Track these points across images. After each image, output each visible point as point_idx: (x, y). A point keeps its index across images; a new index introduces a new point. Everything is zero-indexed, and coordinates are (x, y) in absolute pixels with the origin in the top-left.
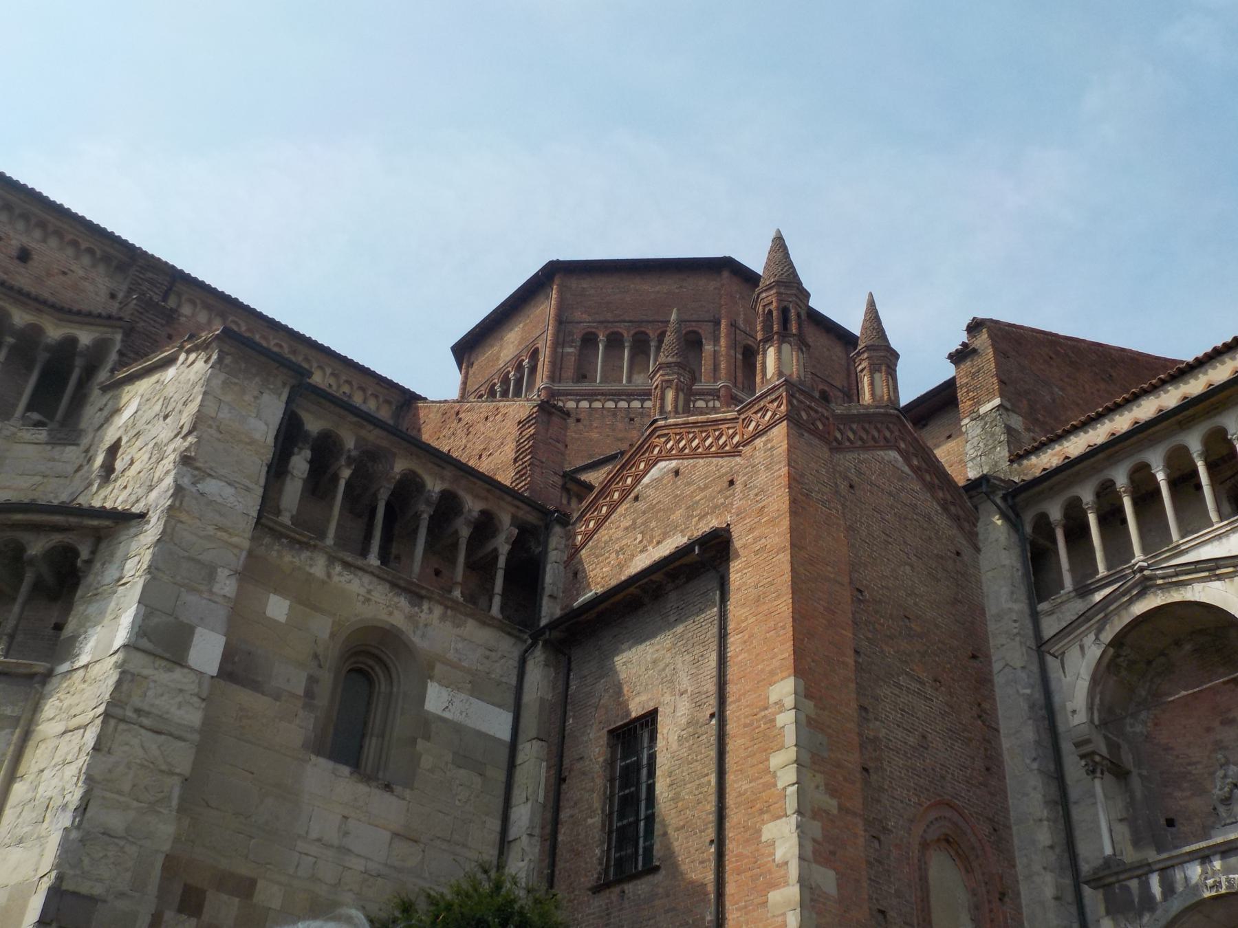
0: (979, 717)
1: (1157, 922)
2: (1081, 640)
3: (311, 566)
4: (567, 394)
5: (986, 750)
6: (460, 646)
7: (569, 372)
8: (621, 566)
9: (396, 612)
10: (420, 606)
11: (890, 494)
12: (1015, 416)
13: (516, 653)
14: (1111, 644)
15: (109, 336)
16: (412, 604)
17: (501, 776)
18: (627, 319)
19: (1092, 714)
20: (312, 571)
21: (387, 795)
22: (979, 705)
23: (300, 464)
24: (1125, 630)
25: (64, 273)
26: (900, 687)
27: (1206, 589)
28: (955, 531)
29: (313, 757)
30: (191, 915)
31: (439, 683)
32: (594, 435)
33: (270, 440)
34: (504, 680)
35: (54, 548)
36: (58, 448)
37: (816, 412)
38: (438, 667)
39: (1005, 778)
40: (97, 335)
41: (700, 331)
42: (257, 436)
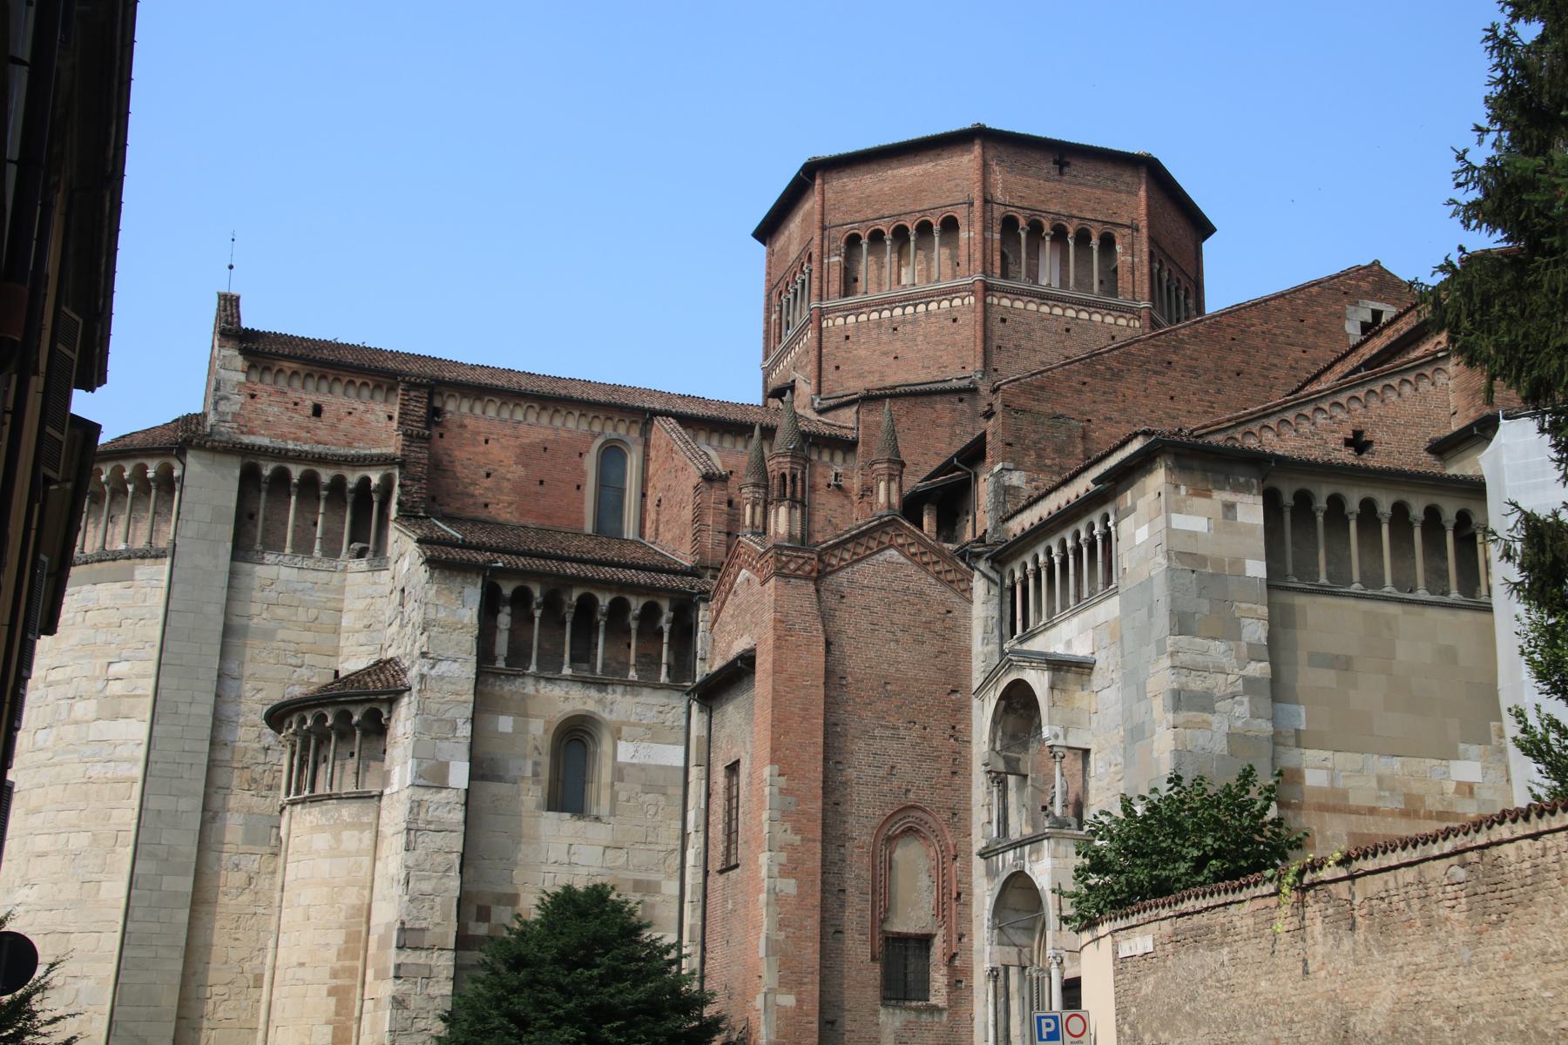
0: (951, 736)
3: (524, 688)
4: (836, 310)
5: (955, 760)
6: (639, 710)
7: (835, 285)
8: (730, 644)
9: (588, 700)
10: (606, 691)
11: (882, 588)
12: (1017, 473)
13: (684, 703)
14: (1001, 698)
15: (390, 471)
16: (600, 691)
17: (680, 791)
18: (887, 213)
19: (995, 743)
20: (525, 691)
21: (598, 824)
22: (954, 728)
23: (504, 619)
25: (350, 413)
26: (874, 738)
28: (950, 594)
29: (545, 814)
30: (484, 922)
31: (626, 741)
32: (863, 352)
33: (475, 620)
34: (676, 724)
35: (368, 711)
36: (376, 573)
37: (803, 558)
38: (625, 730)
39: (970, 775)
40: (382, 472)
41: (956, 215)
42: (466, 620)
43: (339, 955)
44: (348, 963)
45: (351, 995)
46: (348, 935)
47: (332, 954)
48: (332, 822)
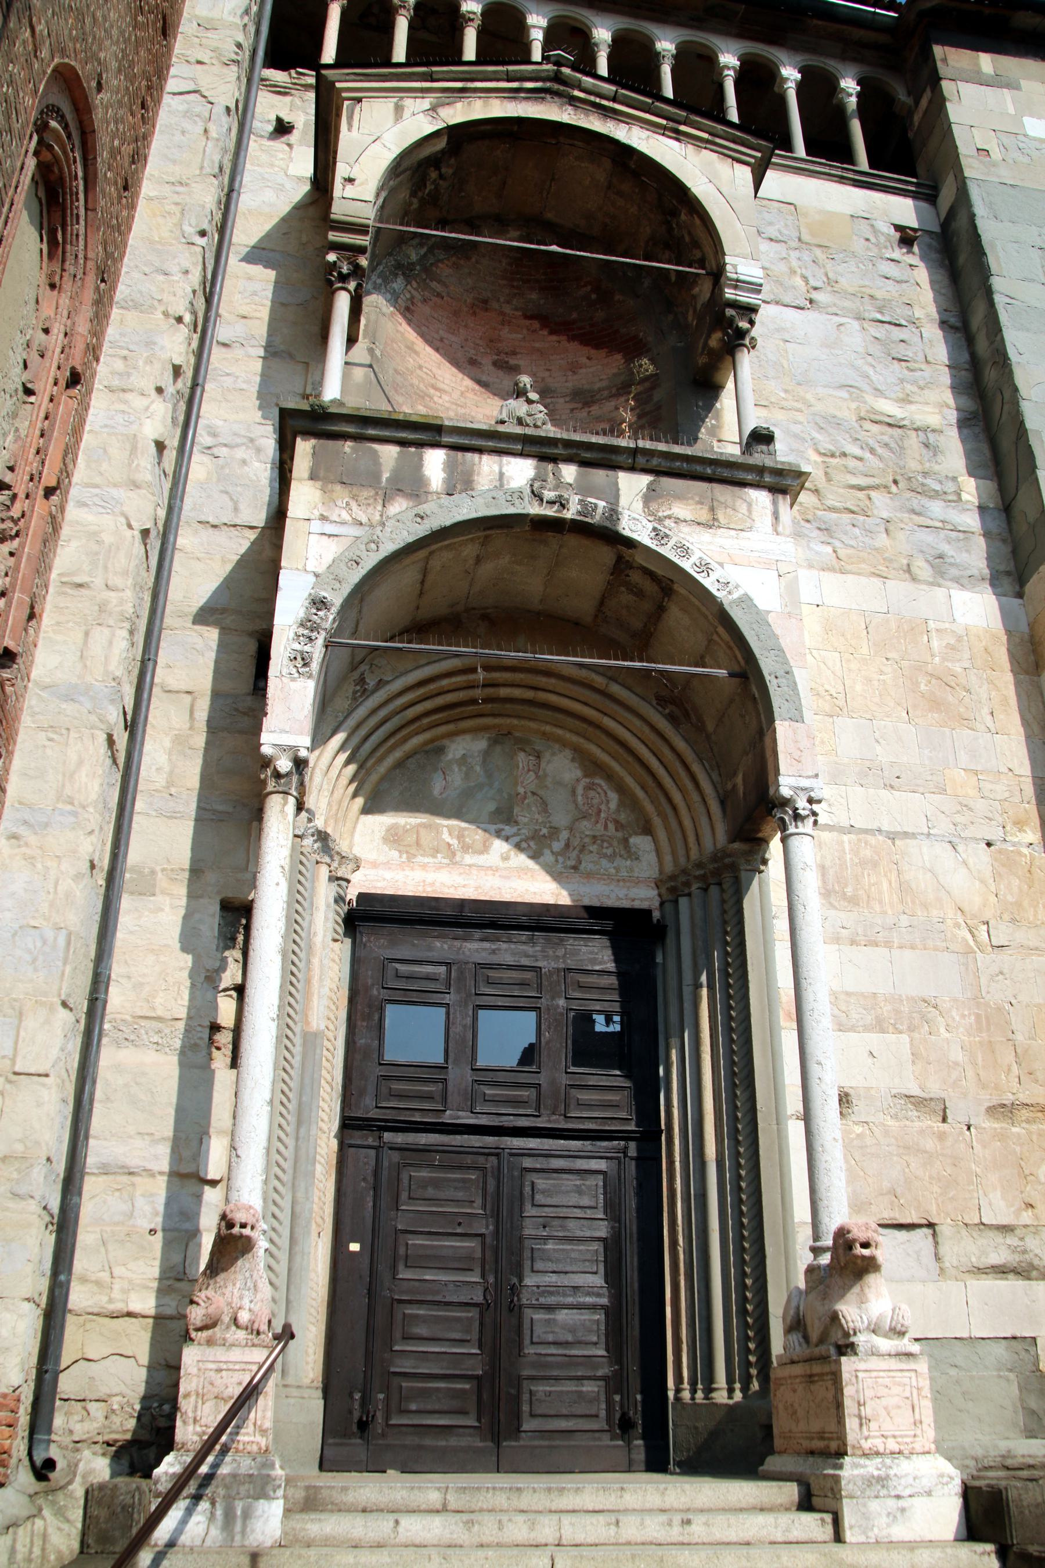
1: (419, 520)
2: (402, 98)
24: (483, 128)
27: (651, 141)
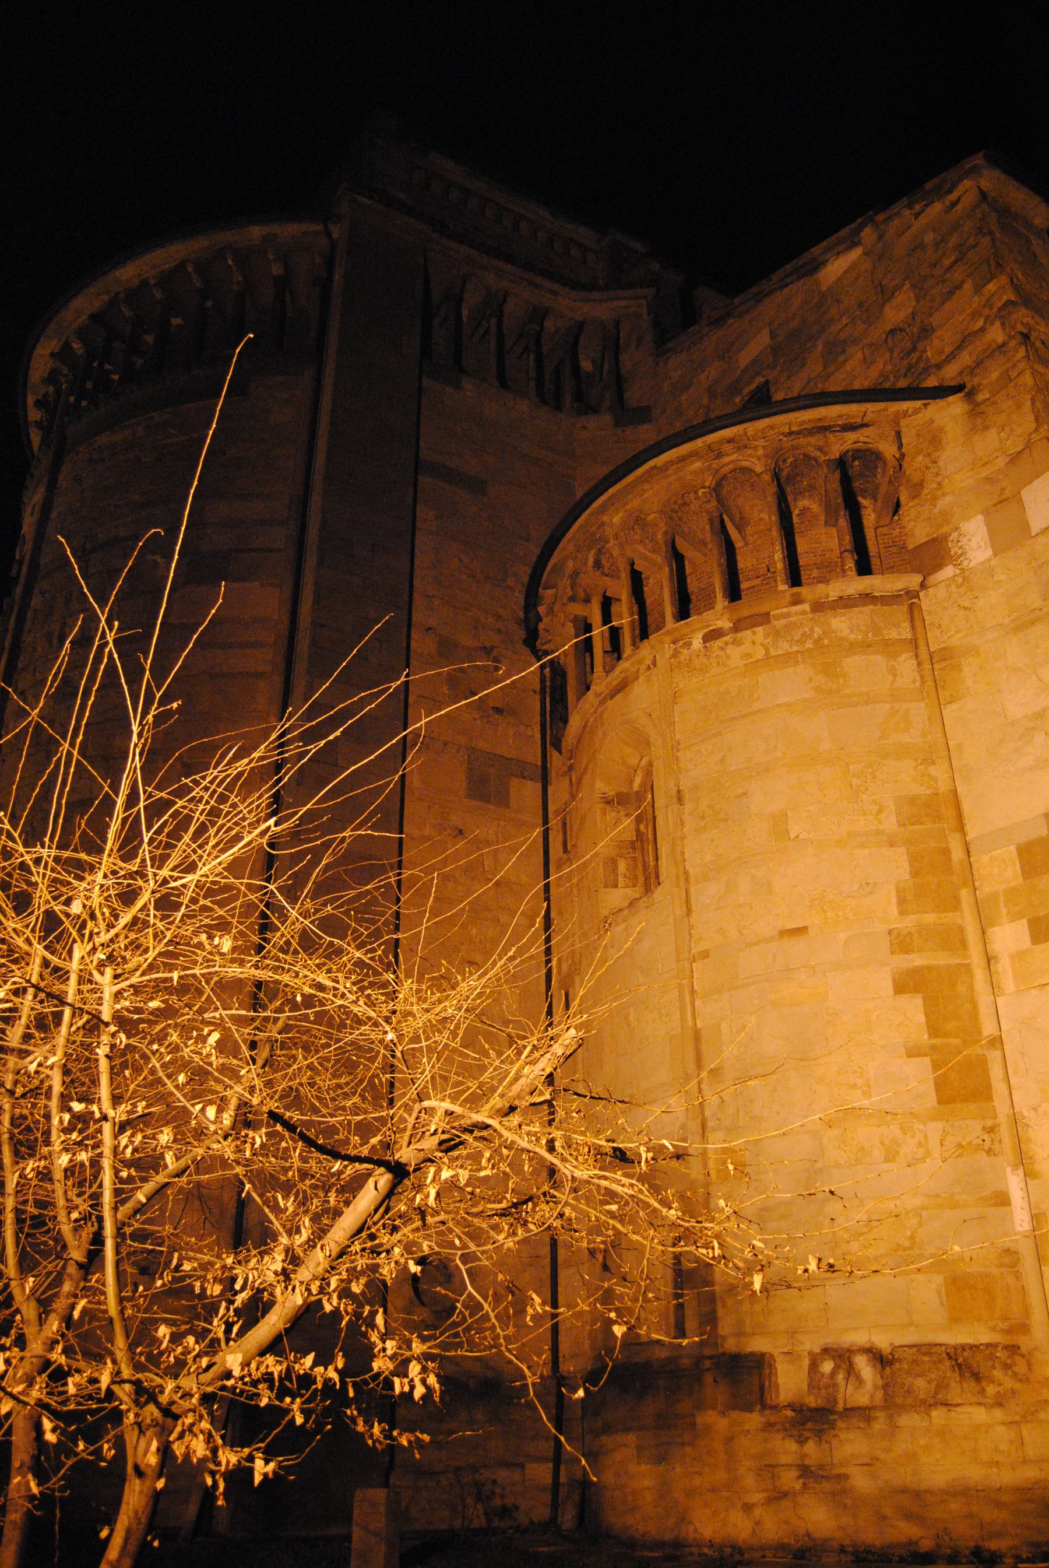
43: (902, 902)
44: (930, 918)
45: (961, 989)
46: (915, 859)
47: (886, 902)
48: (809, 645)
